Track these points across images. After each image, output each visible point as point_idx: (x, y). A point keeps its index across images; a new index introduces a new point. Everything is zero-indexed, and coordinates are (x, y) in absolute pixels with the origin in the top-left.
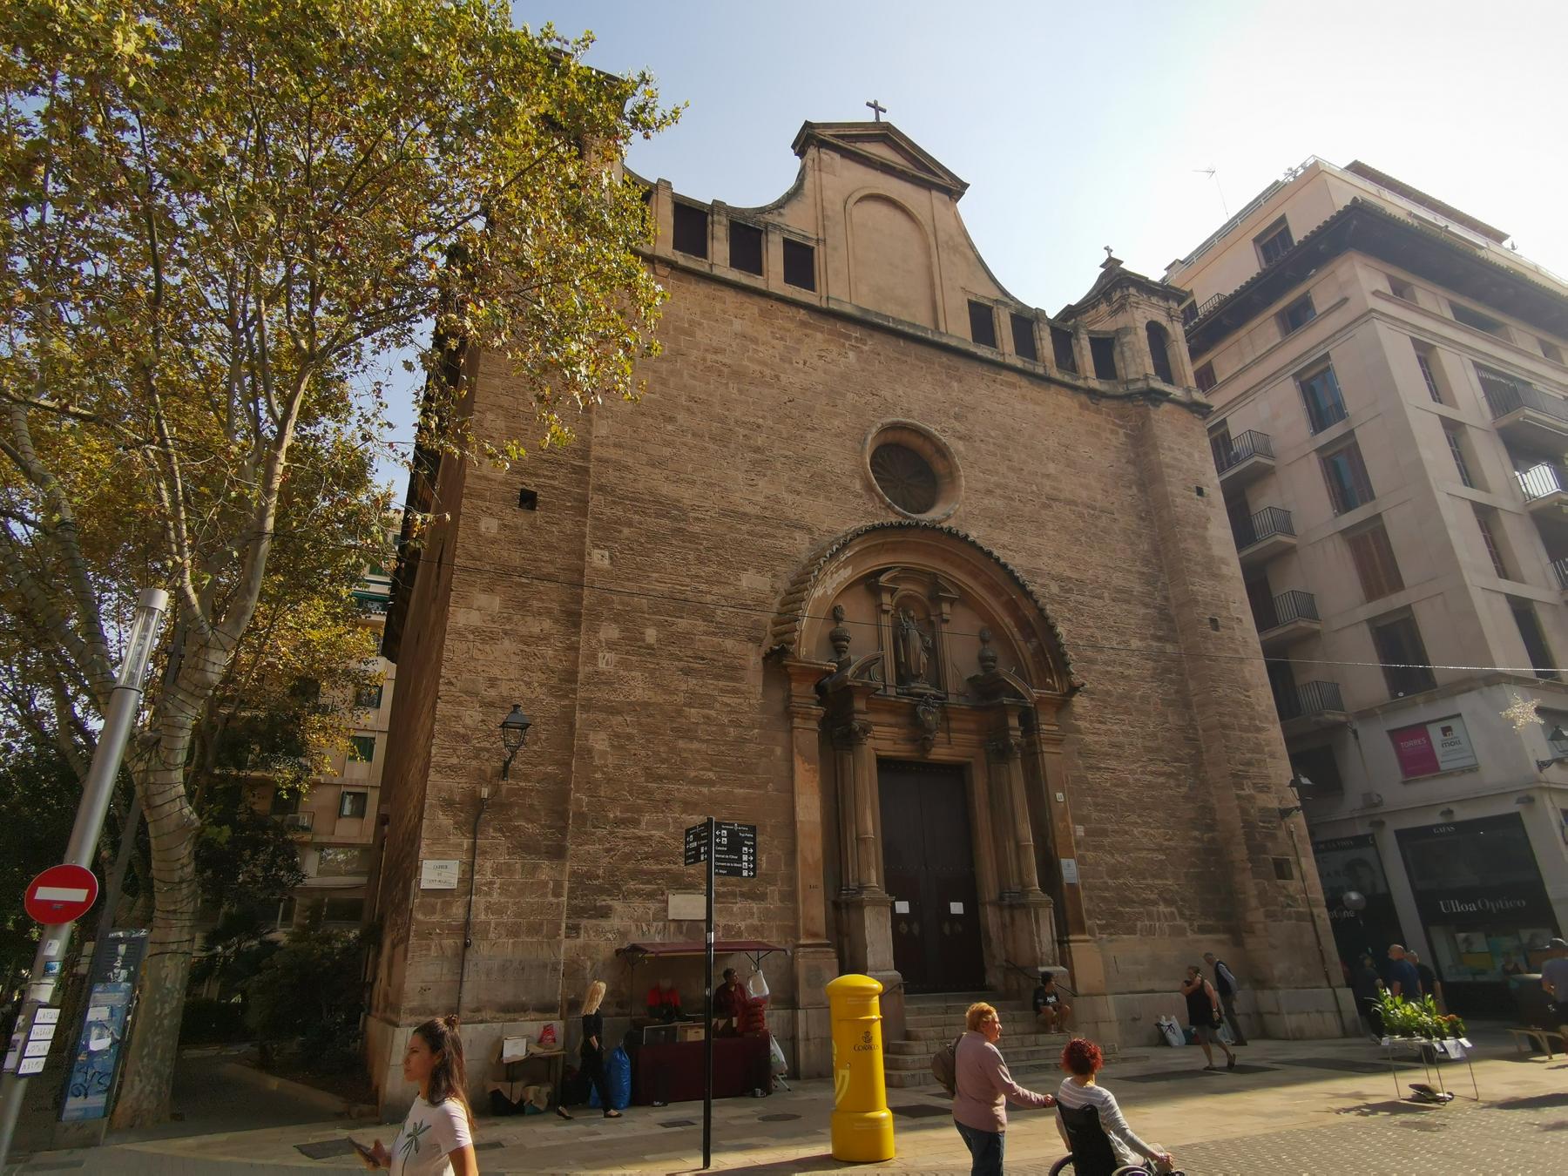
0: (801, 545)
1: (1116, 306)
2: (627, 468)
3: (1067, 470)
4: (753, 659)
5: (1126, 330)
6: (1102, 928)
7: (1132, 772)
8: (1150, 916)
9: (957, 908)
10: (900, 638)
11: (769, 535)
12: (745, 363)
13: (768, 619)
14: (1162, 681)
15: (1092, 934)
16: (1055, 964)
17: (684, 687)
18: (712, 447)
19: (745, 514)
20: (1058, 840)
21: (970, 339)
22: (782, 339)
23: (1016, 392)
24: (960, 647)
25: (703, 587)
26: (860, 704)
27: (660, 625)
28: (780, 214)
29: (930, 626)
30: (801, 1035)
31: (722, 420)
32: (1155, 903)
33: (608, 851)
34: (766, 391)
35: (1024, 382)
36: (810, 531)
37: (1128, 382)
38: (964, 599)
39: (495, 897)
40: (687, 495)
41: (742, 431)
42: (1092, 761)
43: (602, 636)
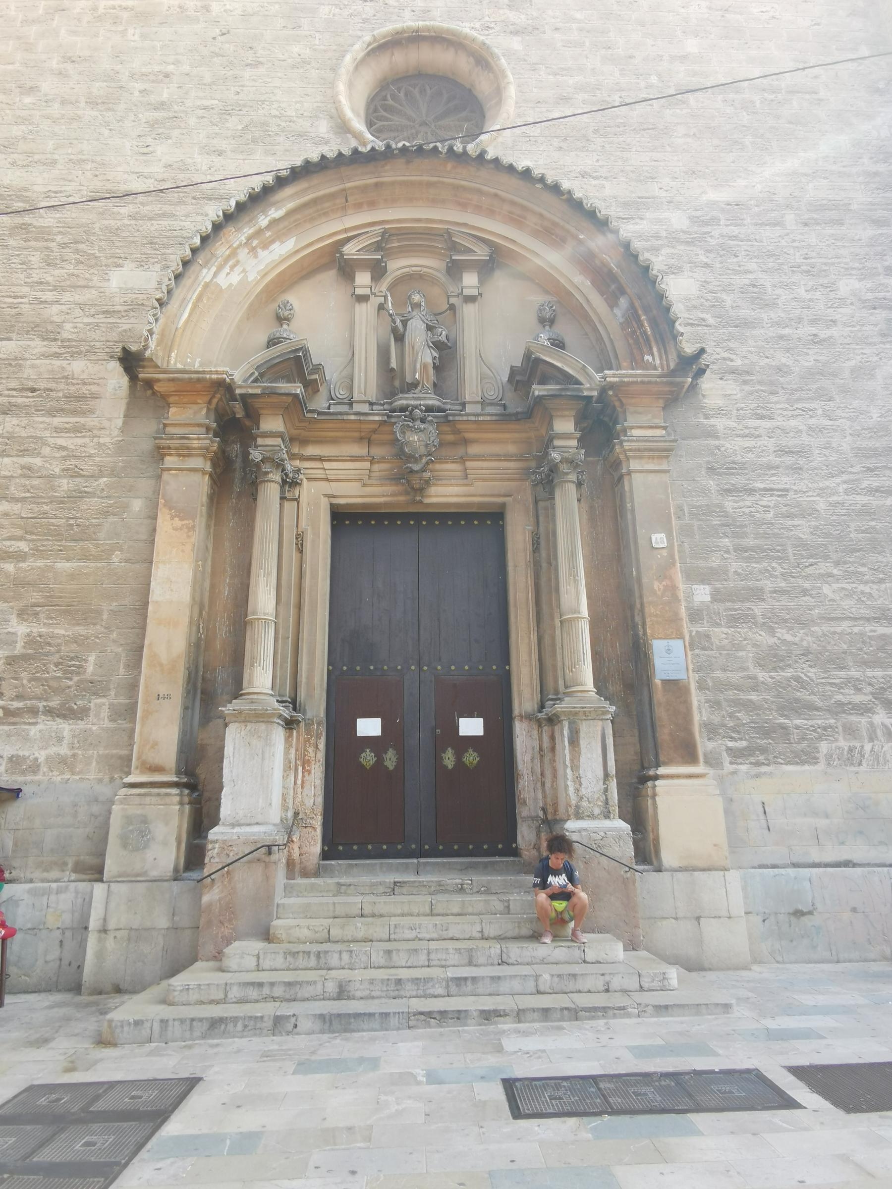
6: (737, 755)
8: (851, 731)
9: (471, 727)
11: (164, 215)
15: (713, 761)
16: (607, 816)
20: (650, 610)
30: (94, 923)
32: (864, 709)
41: (139, 86)
42: (738, 480)
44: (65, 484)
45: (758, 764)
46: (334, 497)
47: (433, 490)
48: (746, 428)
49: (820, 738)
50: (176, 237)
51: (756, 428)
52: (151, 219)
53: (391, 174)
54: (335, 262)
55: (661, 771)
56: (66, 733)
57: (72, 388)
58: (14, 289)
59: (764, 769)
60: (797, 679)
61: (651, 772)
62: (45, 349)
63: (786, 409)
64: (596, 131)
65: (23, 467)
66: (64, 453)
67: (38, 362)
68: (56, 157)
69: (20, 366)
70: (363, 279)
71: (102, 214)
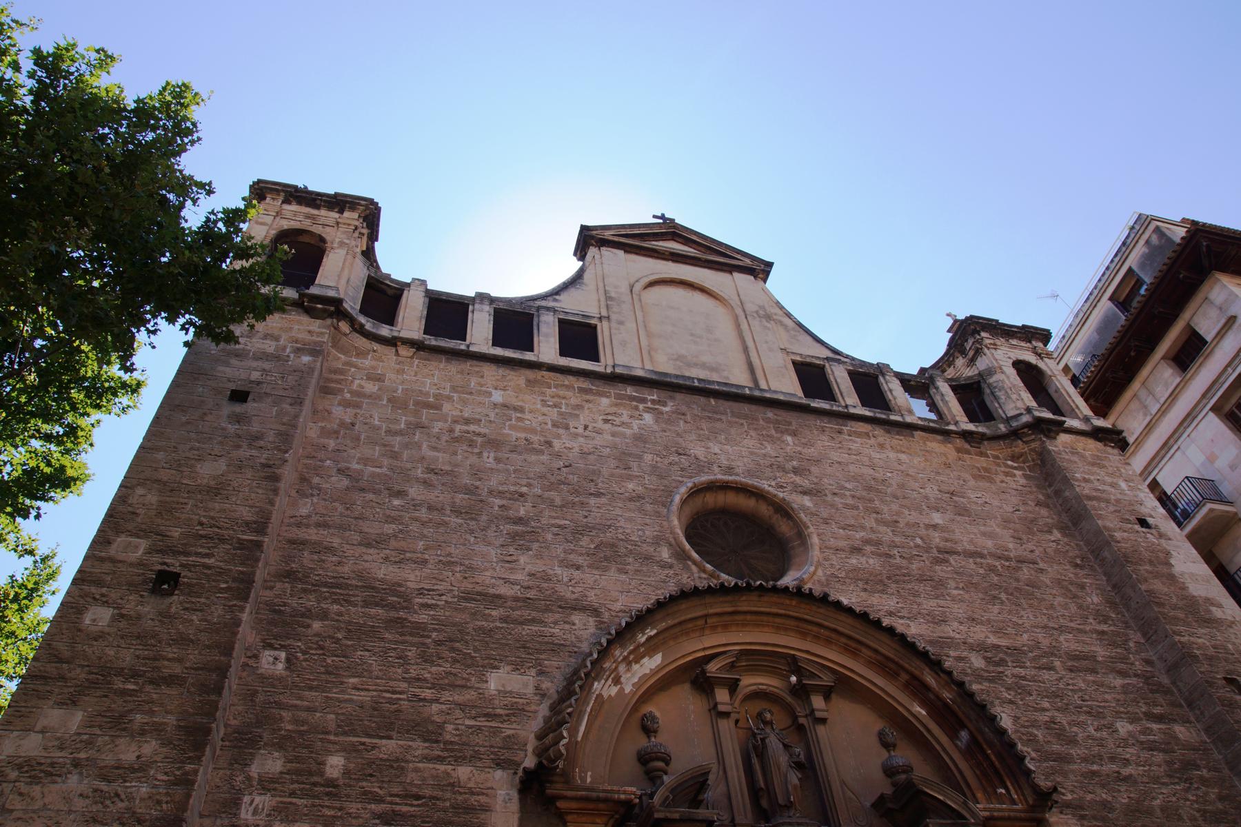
0: (584, 630)
1: (971, 353)
2: (330, 550)
3: (958, 518)
5: (990, 372)
10: (754, 751)
11: (533, 621)
12: (506, 431)
13: (528, 731)
14: (1189, 780)
18: (455, 521)
19: (499, 597)
21: (800, 393)
22: (555, 406)
23: (872, 441)
25: (428, 693)
27: (350, 750)
28: (556, 300)
31: (471, 491)
34: (534, 458)
35: (879, 431)
36: (595, 612)
37: (1008, 420)
38: (843, 686)
40: (412, 577)
41: (498, 502)
43: (254, 770)
50: (547, 643)
52: (522, 623)
53: (746, 604)
54: (696, 677)
57: (460, 798)
58: (392, 683)
62: (426, 751)
64: (889, 578)
67: (420, 765)
68: (427, 557)
69: (403, 768)
70: (722, 695)
71: (474, 614)
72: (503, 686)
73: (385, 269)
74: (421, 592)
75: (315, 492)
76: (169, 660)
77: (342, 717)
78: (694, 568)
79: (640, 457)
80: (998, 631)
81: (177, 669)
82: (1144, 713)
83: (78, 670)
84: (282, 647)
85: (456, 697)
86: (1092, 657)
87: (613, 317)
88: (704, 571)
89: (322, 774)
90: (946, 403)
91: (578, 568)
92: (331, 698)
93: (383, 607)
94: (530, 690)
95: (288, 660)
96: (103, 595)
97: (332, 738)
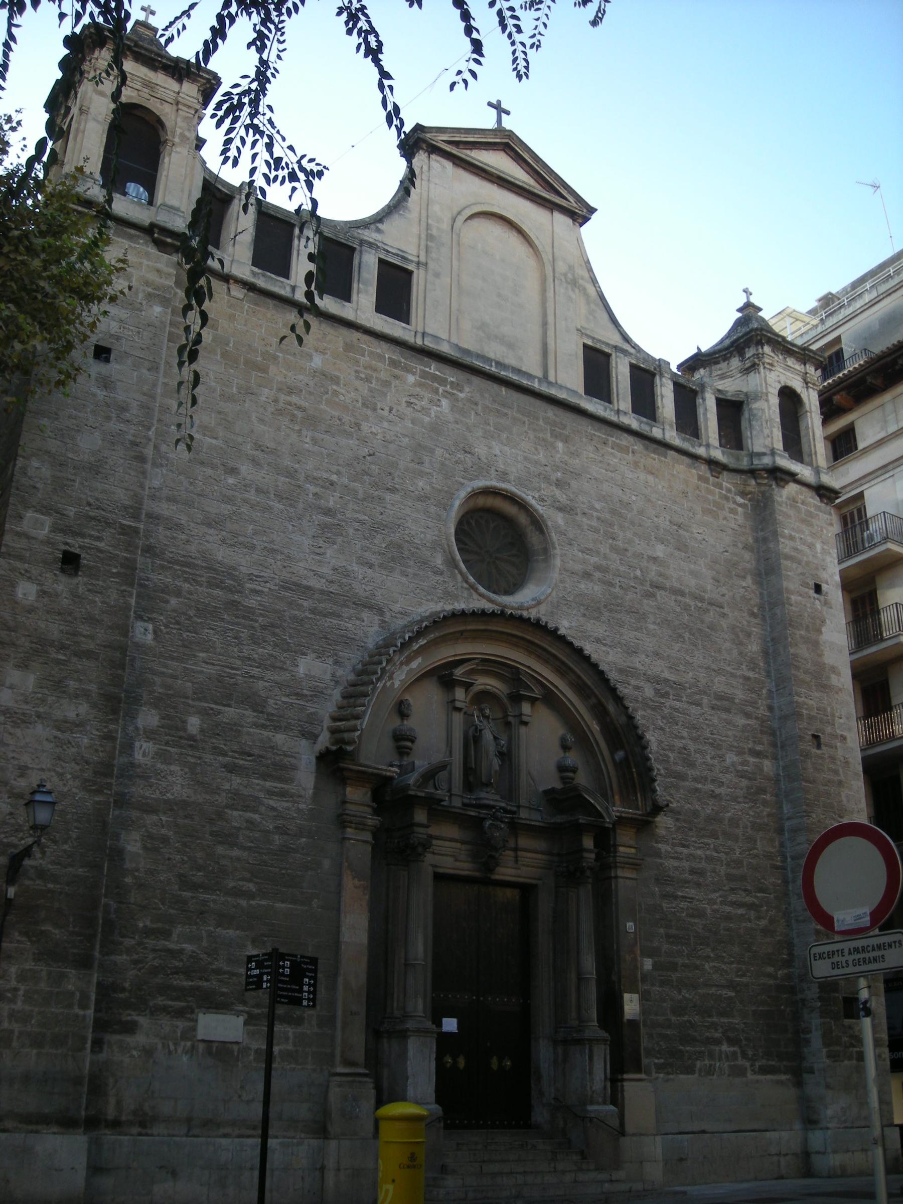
1: (748, 364)
2: (179, 527)
3: (677, 553)
4: (305, 757)
6: (660, 1068)
7: (712, 902)
8: (711, 1056)
10: (473, 740)
11: (333, 614)
12: (323, 407)
13: (326, 709)
15: (648, 1073)
16: (604, 1103)
17: (227, 786)
19: (308, 588)
21: (581, 390)
24: (542, 745)
25: (256, 671)
26: (420, 816)
27: (204, 713)
28: (378, 231)
29: (510, 724)
31: (291, 474)
32: (718, 1042)
33: (135, 962)
34: (343, 441)
36: (380, 612)
37: (752, 455)
38: (550, 699)
39: (19, 1005)
40: (243, 562)
41: (312, 489)
42: (669, 889)
43: (141, 722)
44: (277, 839)
45: (668, 1073)
46: (436, 866)
47: (500, 870)
48: (676, 852)
49: (697, 1059)
50: (342, 636)
51: (681, 853)
52: (325, 616)
55: (626, 1076)
56: (290, 1034)
57: (277, 758)
58: (231, 660)
59: (671, 1077)
60: (690, 1022)
61: (620, 1077)
62: (255, 720)
63: (695, 842)
64: (605, 606)
65: (247, 821)
66: (275, 814)
68: (255, 542)
69: (240, 731)
71: (290, 603)
72: (309, 670)
73: (200, 135)
74: (251, 578)
75: (164, 462)
76: (84, 636)
77: (196, 686)
78: (459, 577)
79: (432, 451)
80: (672, 668)
81: (92, 646)
82: (750, 749)
83: (23, 639)
84: (150, 619)
85: (276, 677)
86: (730, 699)
87: (431, 265)
88: (467, 582)
89: (185, 730)
90: (706, 420)
91: (371, 566)
92: (187, 669)
93: (222, 589)
94: (328, 676)
95: (155, 632)
96: (26, 571)
97: (190, 702)
